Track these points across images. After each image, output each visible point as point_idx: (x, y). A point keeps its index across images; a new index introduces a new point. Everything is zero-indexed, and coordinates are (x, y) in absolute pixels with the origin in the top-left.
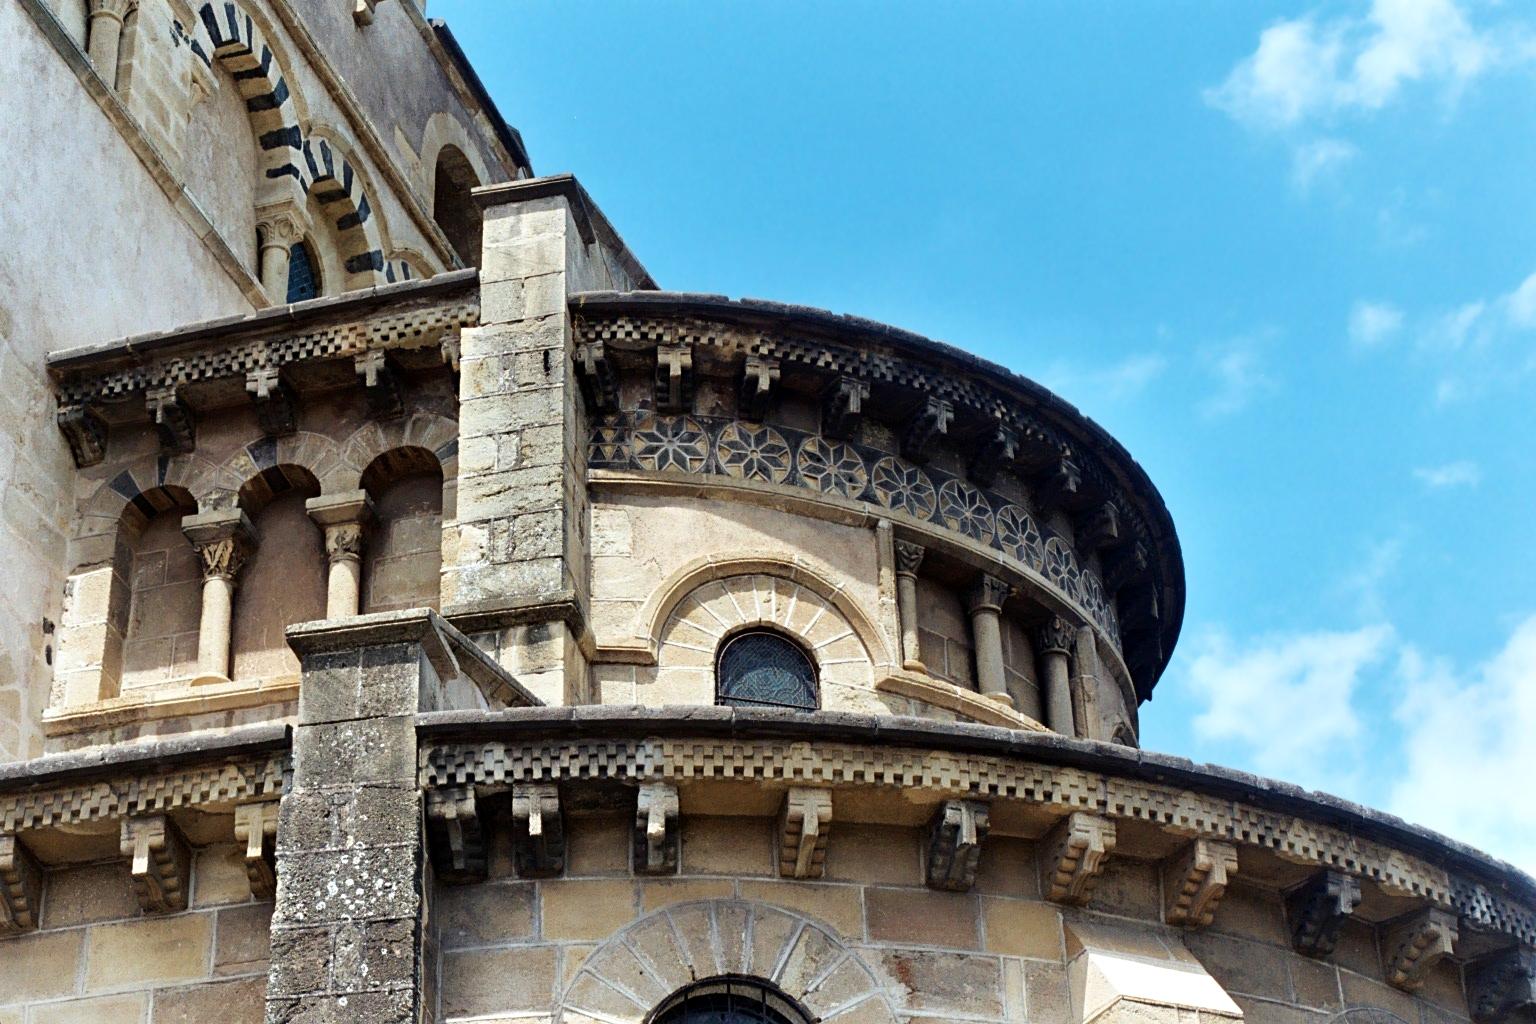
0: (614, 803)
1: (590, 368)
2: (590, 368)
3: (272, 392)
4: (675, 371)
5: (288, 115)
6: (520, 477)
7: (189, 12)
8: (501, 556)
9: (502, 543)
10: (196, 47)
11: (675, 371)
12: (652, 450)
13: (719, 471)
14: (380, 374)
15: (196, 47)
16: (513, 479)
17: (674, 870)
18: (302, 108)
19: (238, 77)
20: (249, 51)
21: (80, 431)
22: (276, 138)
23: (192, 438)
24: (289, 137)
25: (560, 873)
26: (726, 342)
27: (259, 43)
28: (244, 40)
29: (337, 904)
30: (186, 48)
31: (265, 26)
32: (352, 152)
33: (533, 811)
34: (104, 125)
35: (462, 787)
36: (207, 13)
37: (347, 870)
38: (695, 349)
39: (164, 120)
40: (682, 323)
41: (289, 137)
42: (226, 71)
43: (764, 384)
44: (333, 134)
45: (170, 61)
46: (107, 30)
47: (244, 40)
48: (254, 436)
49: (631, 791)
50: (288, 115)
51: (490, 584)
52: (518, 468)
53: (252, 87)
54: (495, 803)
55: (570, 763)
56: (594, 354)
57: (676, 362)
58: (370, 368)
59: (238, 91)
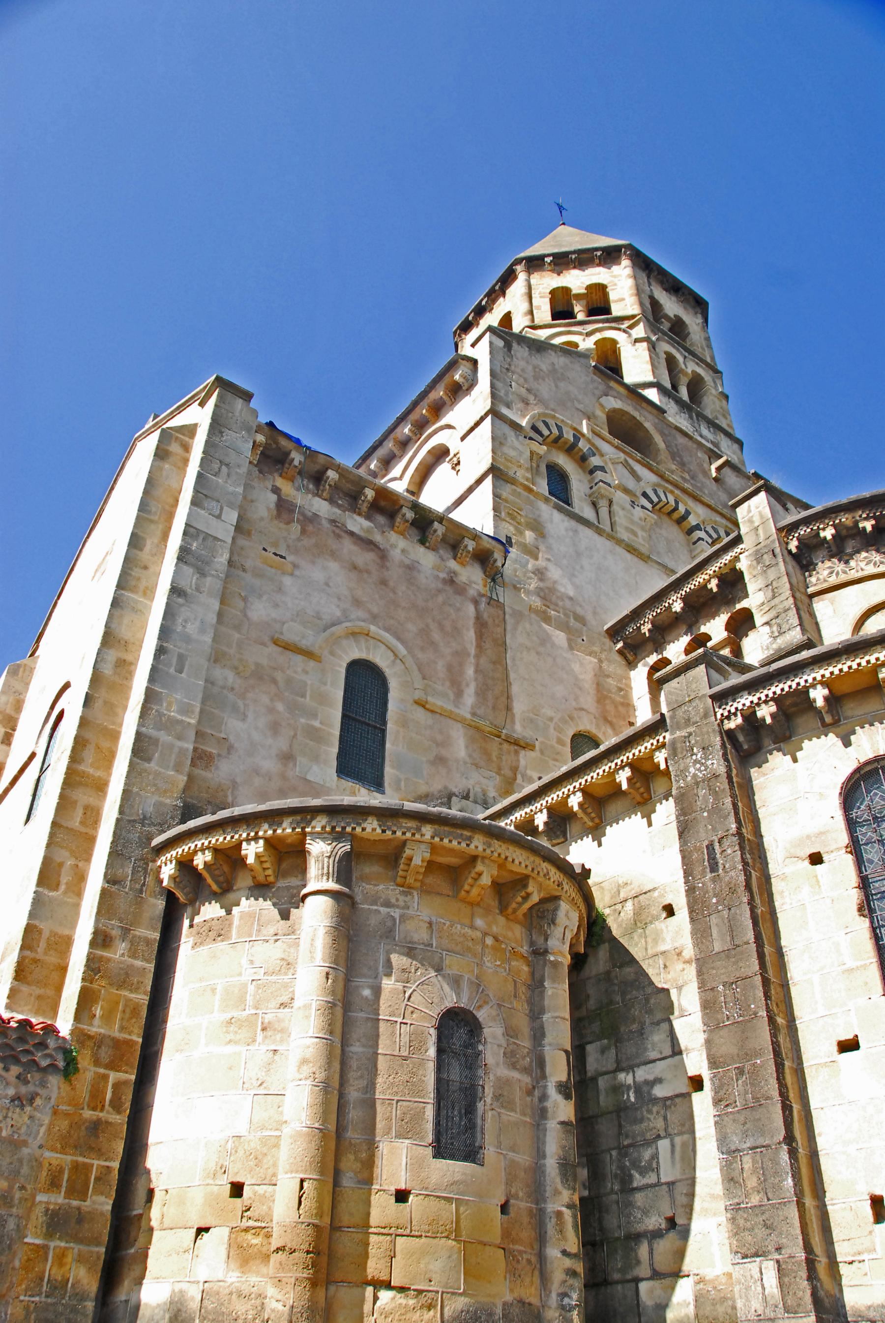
1: (794, 550)
2: (794, 550)
3: (682, 608)
4: (829, 537)
5: (693, 520)
6: (777, 600)
7: (635, 495)
8: (776, 634)
9: (775, 628)
10: (643, 507)
11: (829, 537)
12: (832, 573)
13: (862, 570)
14: (717, 585)
15: (643, 507)
16: (773, 603)
17: (839, 720)
18: (698, 515)
19: (670, 514)
20: (668, 503)
21: (626, 651)
22: (690, 531)
23: (663, 638)
24: (697, 527)
25: (790, 737)
26: (845, 519)
27: (671, 499)
28: (664, 499)
29: (695, 775)
30: (638, 509)
31: (672, 492)
32: (727, 526)
33: (765, 712)
34: (608, 543)
35: (735, 714)
36: (645, 495)
37: (696, 762)
38: (834, 526)
39: (635, 534)
40: (826, 518)
41: (697, 527)
42: (664, 513)
43: (869, 528)
44: (715, 522)
45: (632, 515)
46: (604, 511)
47: (664, 499)
48: (684, 628)
49: (805, 692)
50: (693, 520)
51: (775, 646)
52: (774, 597)
53: (676, 515)
54: (750, 717)
55: (776, 689)
56: (793, 545)
57: (828, 533)
58: (713, 585)
59: (671, 519)
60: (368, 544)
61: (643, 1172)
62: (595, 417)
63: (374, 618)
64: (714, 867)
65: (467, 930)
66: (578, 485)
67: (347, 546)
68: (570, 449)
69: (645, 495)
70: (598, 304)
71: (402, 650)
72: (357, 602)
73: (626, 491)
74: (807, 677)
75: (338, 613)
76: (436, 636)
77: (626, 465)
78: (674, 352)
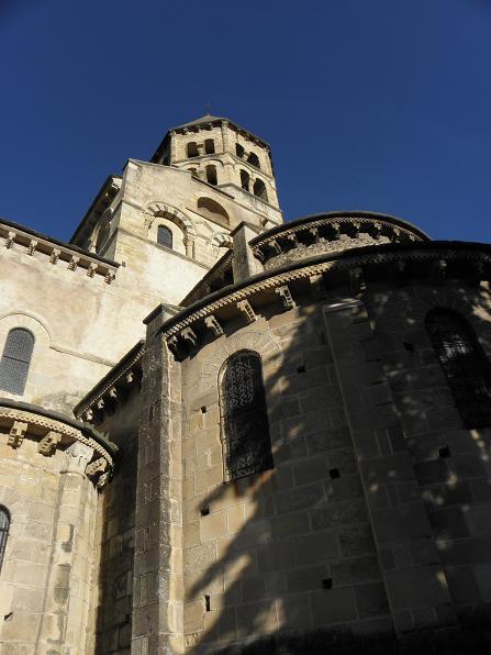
0: (199, 327)
36: (216, 239)
46: (190, 248)
60: (30, 269)
61: (121, 590)
62: (190, 201)
63: (30, 306)
64: (151, 420)
65: (13, 462)
66: (178, 235)
67: (20, 272)
68: (173, 218)
69: (216, 239)
70: (210, 147)
71: (44, 321)
72: (21, 299)
73: (203, 237)
74: (204, 311)
75: (8, 304)
76: (69, 313)
77: (206, 225)
78: (246, 169)
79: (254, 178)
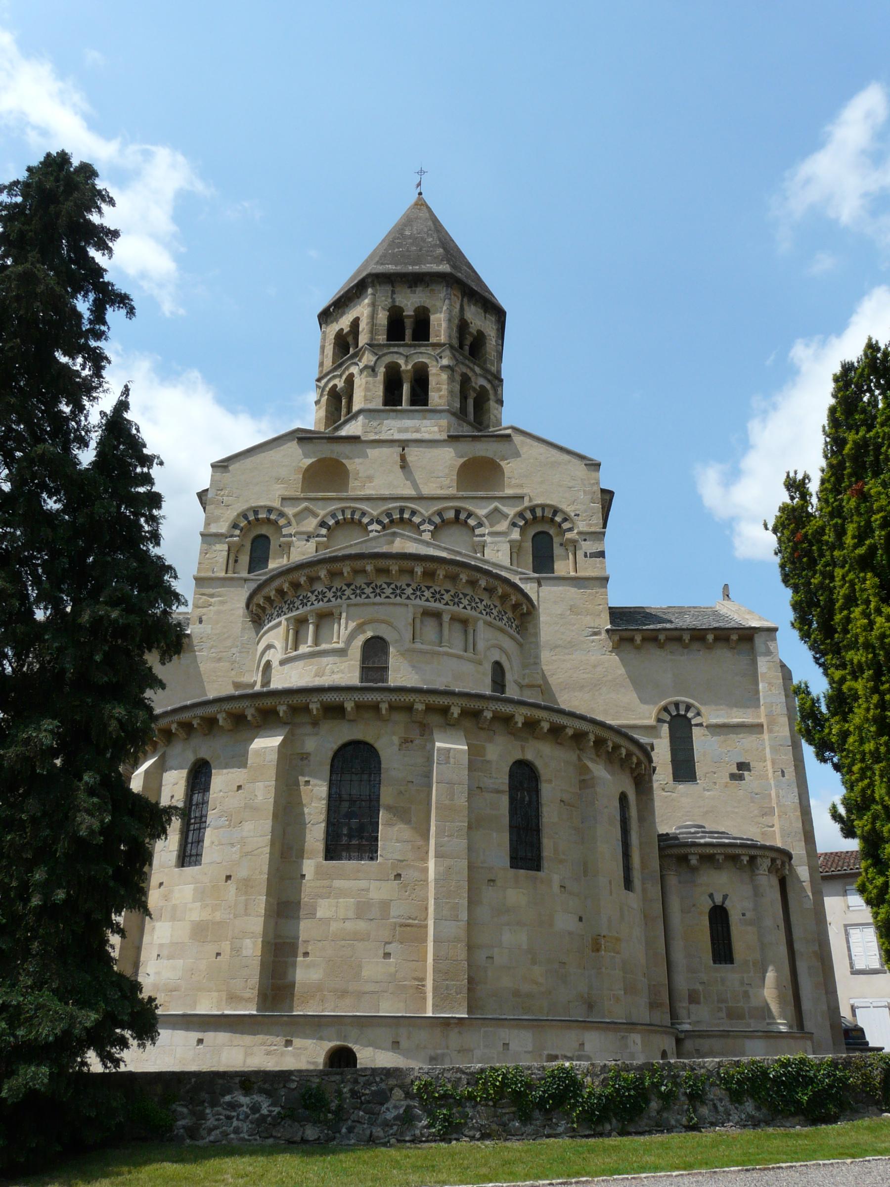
79: (409, 367)
